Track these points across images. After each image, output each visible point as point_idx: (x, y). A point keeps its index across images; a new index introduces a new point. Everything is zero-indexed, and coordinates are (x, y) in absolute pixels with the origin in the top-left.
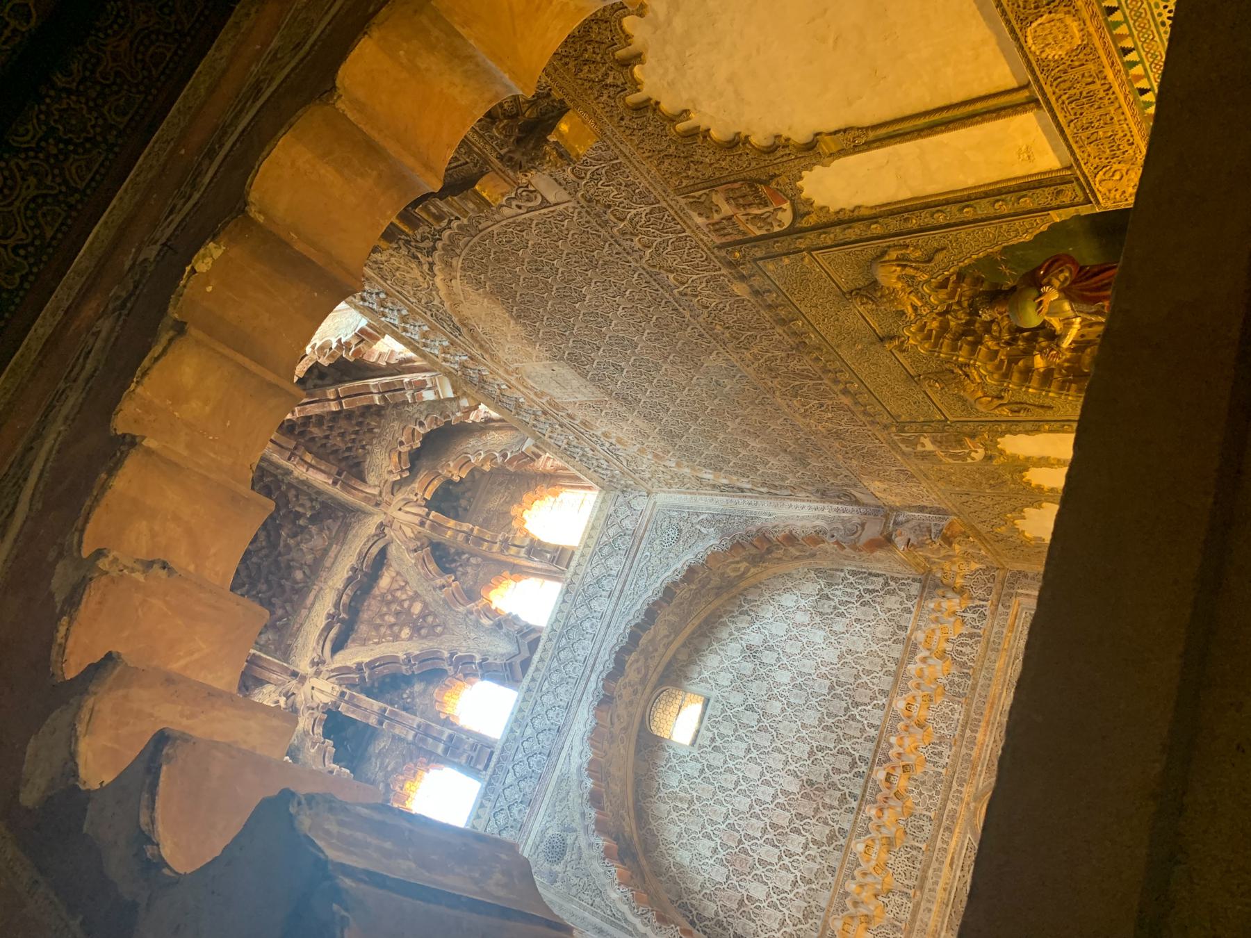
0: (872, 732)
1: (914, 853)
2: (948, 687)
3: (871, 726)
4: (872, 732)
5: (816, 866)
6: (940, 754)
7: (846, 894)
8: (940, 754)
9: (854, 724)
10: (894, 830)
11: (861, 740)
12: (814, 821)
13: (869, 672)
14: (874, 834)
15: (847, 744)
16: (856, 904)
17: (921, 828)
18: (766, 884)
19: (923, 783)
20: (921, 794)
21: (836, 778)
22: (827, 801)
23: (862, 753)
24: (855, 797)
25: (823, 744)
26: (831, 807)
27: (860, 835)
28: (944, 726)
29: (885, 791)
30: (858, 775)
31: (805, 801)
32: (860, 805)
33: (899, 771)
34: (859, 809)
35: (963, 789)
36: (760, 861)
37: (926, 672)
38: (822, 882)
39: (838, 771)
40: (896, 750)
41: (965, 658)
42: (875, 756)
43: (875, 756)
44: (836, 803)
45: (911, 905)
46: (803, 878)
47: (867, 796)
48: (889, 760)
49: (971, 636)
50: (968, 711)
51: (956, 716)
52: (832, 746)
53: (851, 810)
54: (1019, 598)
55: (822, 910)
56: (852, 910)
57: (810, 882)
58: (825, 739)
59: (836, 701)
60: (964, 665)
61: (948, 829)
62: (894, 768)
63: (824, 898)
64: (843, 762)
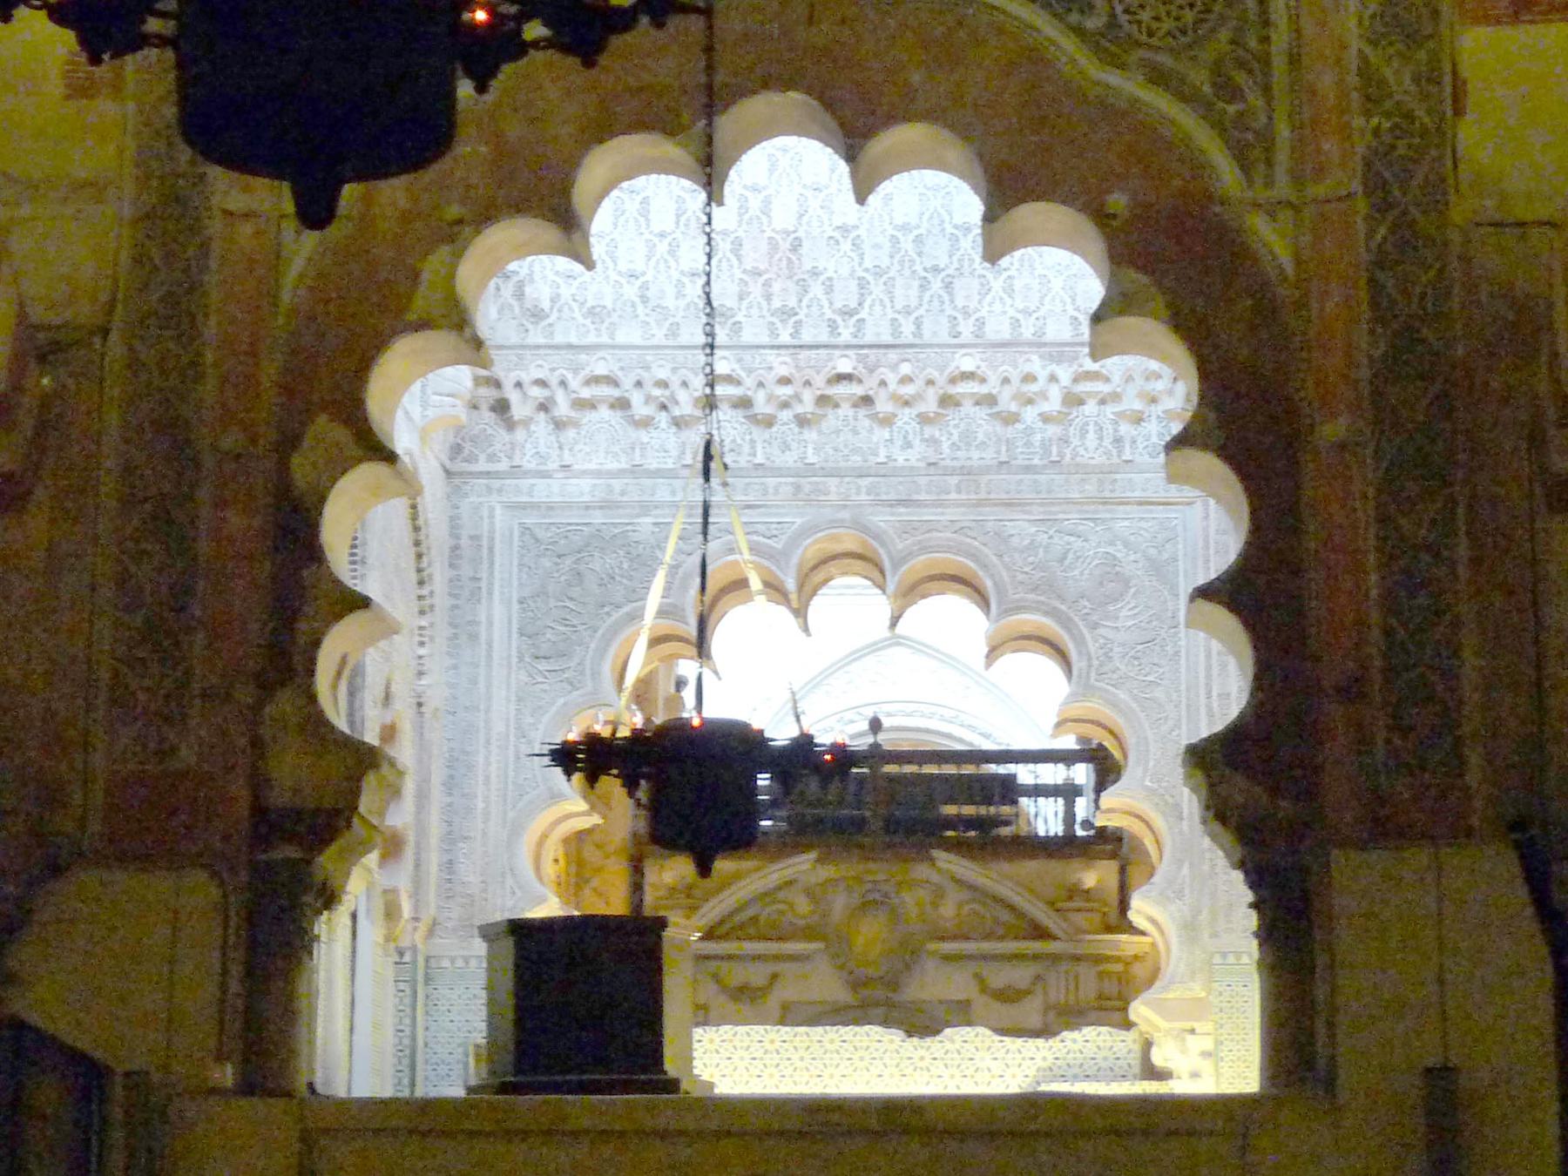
0: (907, 328)
1: (746, 449)
2: (1019, 426)
3: (918, 324)
4: (907, 328)
5: (670, 302)
6: (908, 445)
7: (647, 368)
8: (908, 445)
9: (914, 292)
10: (769, 410)
11: (890, 314)
12: (738, 274)
13: (1009, 291)
14: (749, 382)
15: (877, 290)
16: (639, 384)
17: (786, 447)
18: (615, 226)
19: (855, 432)
20: (838, 432)
21: (817, 289)
22: (776, 287)
23: (870, 322)
24: (796, 333)
25: (866, 247)
26: (768, 298)
27: (740, 360)
28: (955, 437)
29: (819, 381)
30: (833, 326)
31: (764, 247)
32: (787, 347)
33: (858, 390)
34: (779, 347)
35: (863, 497)
36: (645, 201)
37: (1033, 388)
38: (651, 320)
39: (829, 289)
40: (892, 379)
41: (1075, 442)
42: (871, 346)
43: (871, 346)
44: (777, 303)
45: (670, 461)
46: (645, 287)
47: (804, 354)
48: (871, 371)
49: (1118, 441)
50: (986, 470)
51: (975, 455)
52: (868, 264)
53: (774, 333)
54: (1198, 506)
55: (612, 336)
56: (627, 382)
57: (645, 299)
58: (877, 246)
59: (945, 244)
60: (1064, 440)
61: (798, 488)
62: (860, 381)
63: (629, 334)
64: (846, 295)
